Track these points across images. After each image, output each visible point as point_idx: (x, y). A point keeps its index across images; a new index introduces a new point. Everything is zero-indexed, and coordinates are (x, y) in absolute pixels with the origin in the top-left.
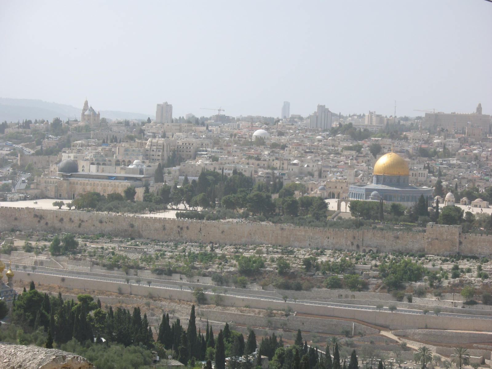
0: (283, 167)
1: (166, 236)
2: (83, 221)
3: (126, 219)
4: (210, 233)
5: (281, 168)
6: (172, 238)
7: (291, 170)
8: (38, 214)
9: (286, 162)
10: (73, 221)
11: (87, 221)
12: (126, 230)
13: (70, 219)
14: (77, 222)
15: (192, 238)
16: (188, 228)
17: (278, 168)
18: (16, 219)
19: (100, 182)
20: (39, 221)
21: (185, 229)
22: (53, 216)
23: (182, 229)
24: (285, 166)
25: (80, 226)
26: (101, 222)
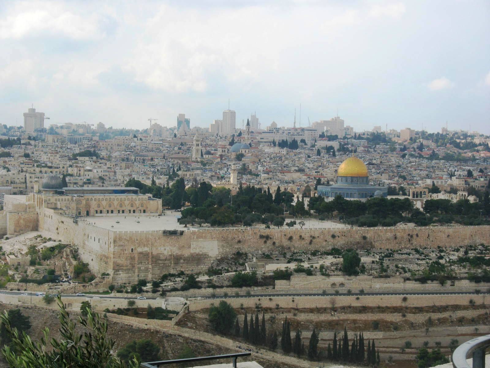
0: (80, 174)
1: (397, 245)
2: (314, 238)
3: (358, 232)
4: (437, 238)
5: (78, 175)
6: (403, 246)
7: (87, 175)
8: (264, 235)
9: (82, 169)
10: (303, 239)
11: (318, 237)
12: (358, 242)
13: (301, 236)
14: (308, 239)
15: (422, 244)
16: (417, 235)
17: (75, 175)
18: (239, 242)
19: (116, 196)
20: (265, 242)
21: (415, 237)
22: (281, 235)
23: (412, 236)
24: (82, 173)
25: (311, 243)
26: (333, 236)
